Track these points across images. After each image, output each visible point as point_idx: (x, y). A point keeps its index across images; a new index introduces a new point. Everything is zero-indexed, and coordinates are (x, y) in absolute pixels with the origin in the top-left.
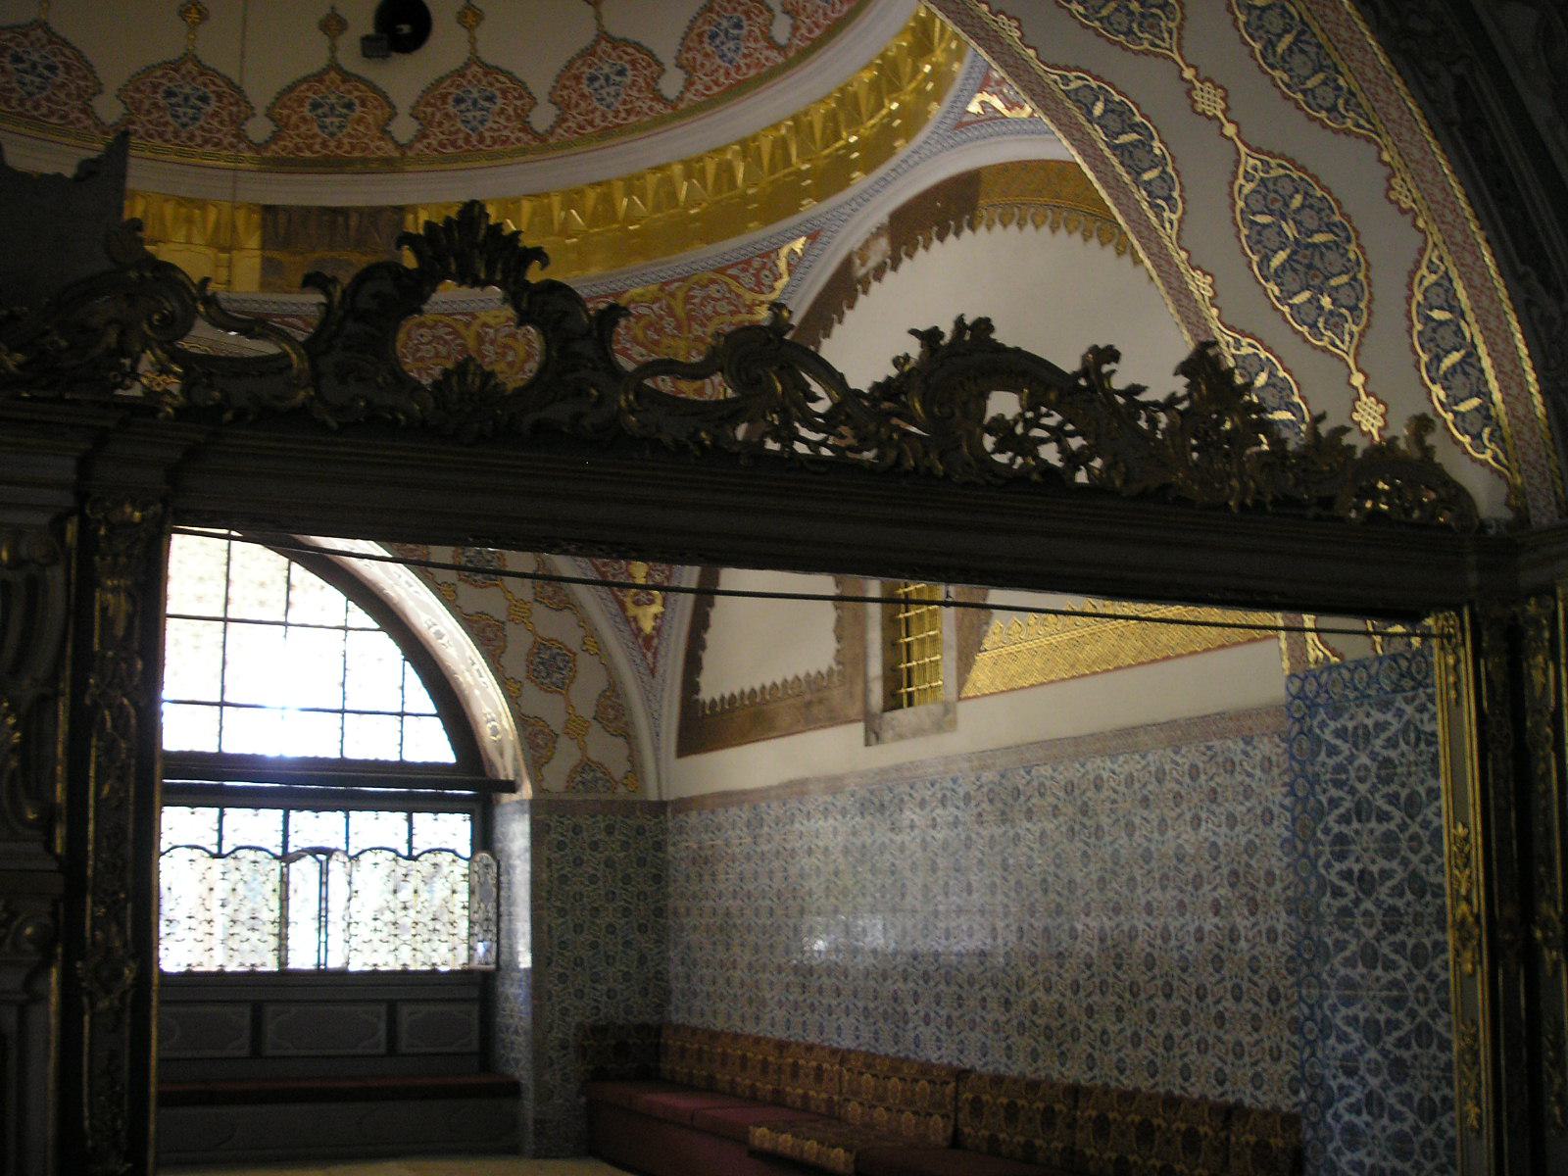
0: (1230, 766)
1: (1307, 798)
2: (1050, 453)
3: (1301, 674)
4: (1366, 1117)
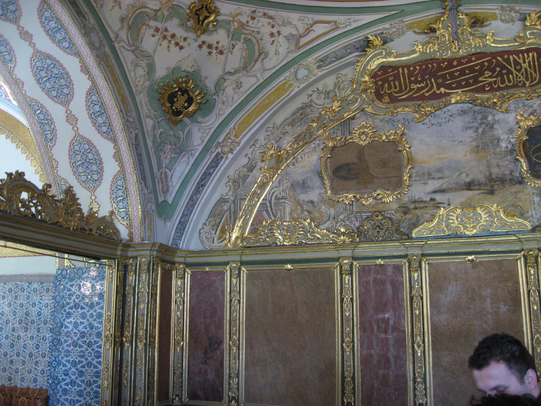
0: (23, 289)
1: (59, 302)
2: (33, 210)
3: (62, 269)
4: (70, 386)
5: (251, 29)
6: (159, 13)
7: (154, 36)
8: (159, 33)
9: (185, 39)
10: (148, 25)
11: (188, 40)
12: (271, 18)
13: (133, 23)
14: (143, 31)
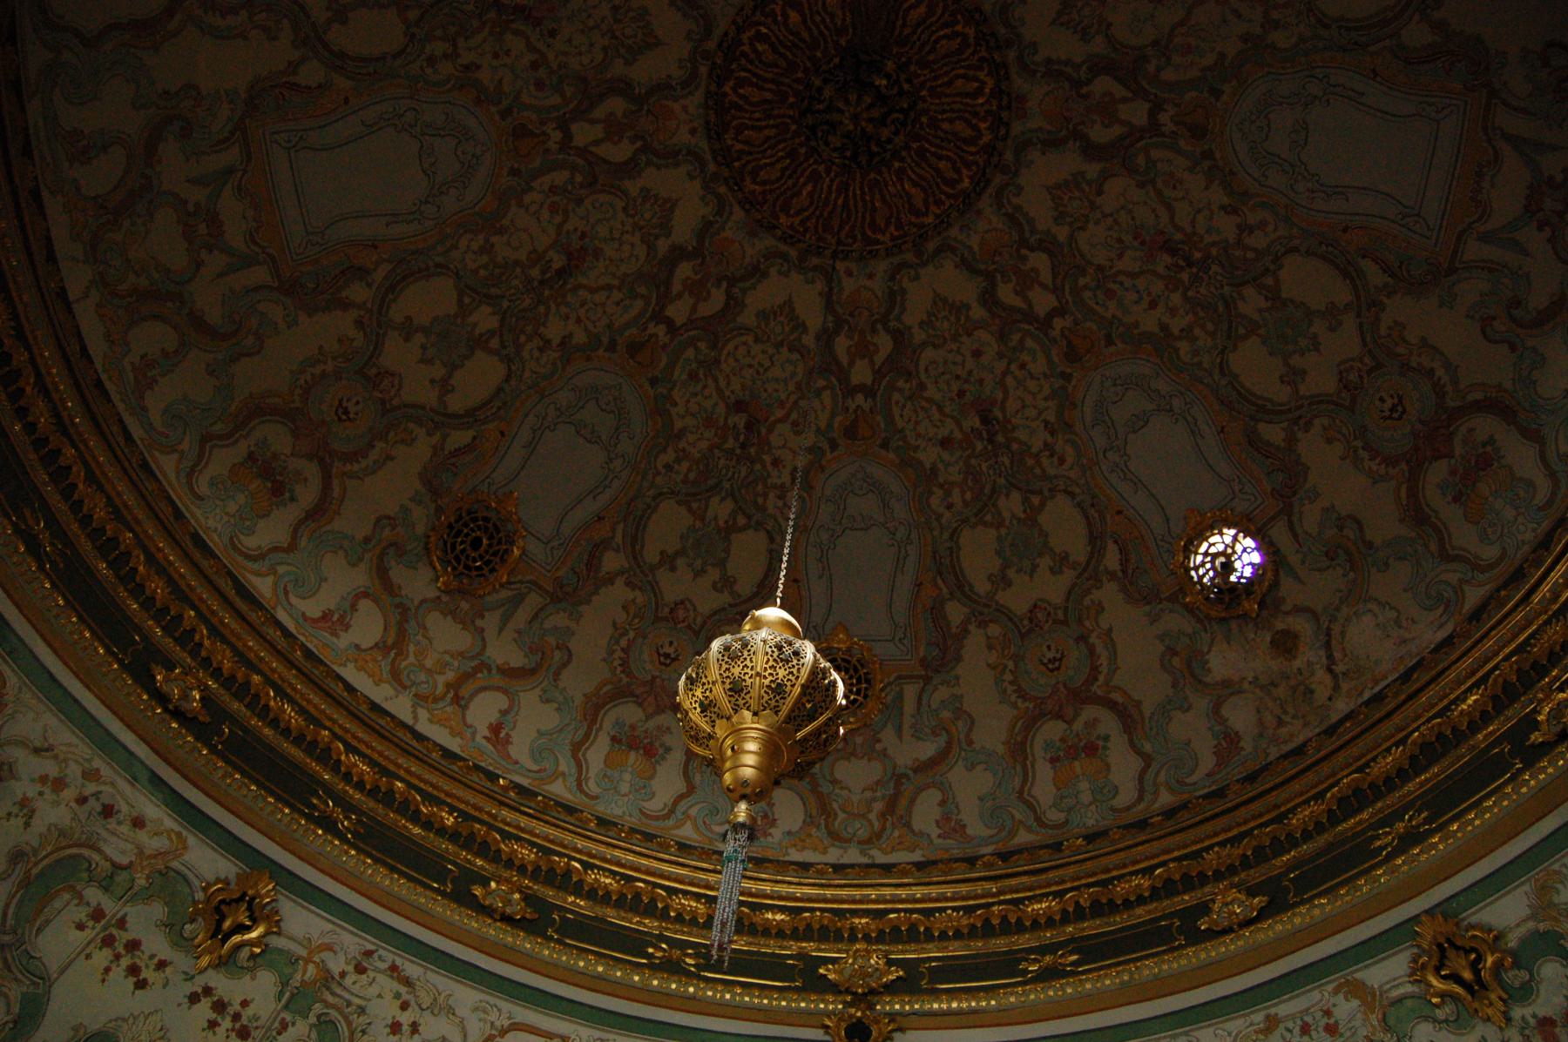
5: (346, 995)
6: (122, 877)
7: (81, 927)
8: (99, 926)
9: (162, 965)
10: (80, 897)
11: (168, 970)
12: (407, 982)
13: (41, 874)
14: (57, 904)
